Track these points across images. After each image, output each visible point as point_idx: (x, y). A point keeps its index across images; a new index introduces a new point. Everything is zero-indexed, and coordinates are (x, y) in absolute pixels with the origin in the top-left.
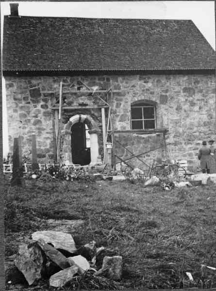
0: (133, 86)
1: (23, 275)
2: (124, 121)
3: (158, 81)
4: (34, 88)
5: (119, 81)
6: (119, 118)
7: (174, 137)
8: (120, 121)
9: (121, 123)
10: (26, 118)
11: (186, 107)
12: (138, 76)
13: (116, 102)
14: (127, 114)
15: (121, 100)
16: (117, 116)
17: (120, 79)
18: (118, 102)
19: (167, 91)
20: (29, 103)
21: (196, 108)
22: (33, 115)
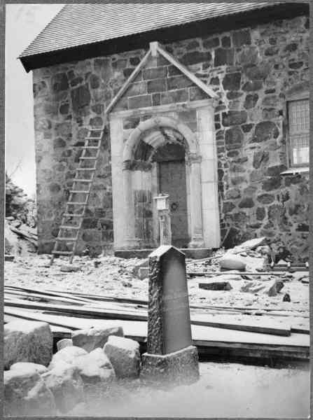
2: (266, 139)
4: (79, 85)
5: (253, 41)
8: (254, 140)
9: (257, 144)
10: (65, 149)
13: (245, 94)
14: (273, 120)
15: (258, 87)
17: (255, 34)
18: (251, 93)
20: (70, 117)
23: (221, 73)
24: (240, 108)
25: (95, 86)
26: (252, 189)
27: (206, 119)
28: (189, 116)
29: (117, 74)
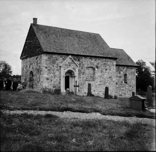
0: (87, 61)
1: (149, 118)
3: (96, 60)
6: (82, 73)
7: (100, 82)
8: (82, 74)
11: (104, 71)
12: (89, 57)
16: (82, 72)
17: (83, 58)
21: (107, 71)
22: (52, 70)
23: (78, 63)
24: (81, 69)
25: (57, 60)
26: (82, 82)
29: (61, 59)
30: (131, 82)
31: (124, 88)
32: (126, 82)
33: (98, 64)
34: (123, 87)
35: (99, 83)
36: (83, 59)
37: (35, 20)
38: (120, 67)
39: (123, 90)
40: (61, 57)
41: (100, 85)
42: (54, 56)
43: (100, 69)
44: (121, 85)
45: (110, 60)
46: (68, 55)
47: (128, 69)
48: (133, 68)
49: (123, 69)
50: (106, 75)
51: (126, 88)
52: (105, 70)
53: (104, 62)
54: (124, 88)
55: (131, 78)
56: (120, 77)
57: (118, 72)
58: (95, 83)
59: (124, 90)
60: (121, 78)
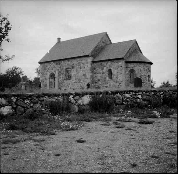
0: (65, 64)
3: (72, 61)
7: (75, 80)
11: (79, 69)
17: (63, 61)
19: (74, 64)
21: (82, 70)
23: (59, 66)
25: (47, 67)
26: (61, 82)
27: (57, 72)
28: (55, 72)
30: (117, 77)
31: (108, 85)
32: (111, 78)
33: (74, 64)
34: (107, 84)
35: (74, 81)
36: (62, 63)
37: (59, 39)
38: (103, 63)
39: (107, 87)
40: (49, 64)
41: (75, 83)
42: (45, 64)
43: (75, 69)
44: (105, 82)
45: (85, 58)
46: (50, 62)
47: (113, 64)
48: (118, 61)
49: (107, 64)
50: (81, 74)
51: (110, 85)
52: (79, 68)
53: (79, 62)
54: (108, 85)
55: (117, 73)
56: (103, 73)
57: (101, 68)
58: (71, 81)
59: (108, 87)
60: (104, 74)
